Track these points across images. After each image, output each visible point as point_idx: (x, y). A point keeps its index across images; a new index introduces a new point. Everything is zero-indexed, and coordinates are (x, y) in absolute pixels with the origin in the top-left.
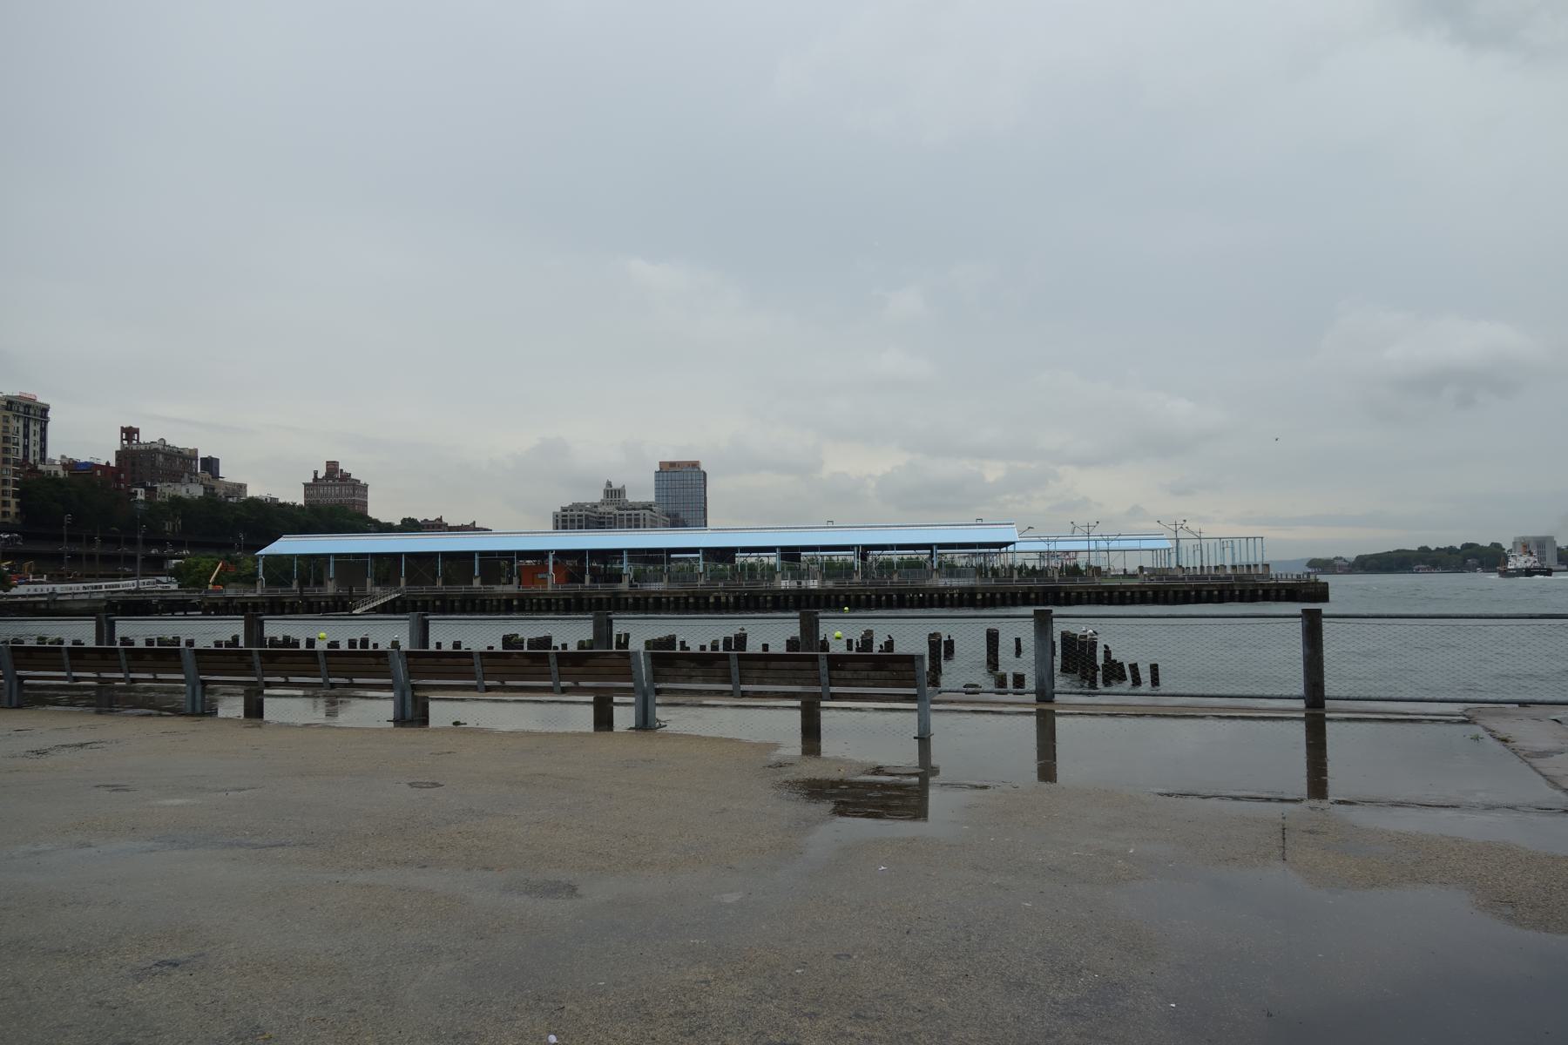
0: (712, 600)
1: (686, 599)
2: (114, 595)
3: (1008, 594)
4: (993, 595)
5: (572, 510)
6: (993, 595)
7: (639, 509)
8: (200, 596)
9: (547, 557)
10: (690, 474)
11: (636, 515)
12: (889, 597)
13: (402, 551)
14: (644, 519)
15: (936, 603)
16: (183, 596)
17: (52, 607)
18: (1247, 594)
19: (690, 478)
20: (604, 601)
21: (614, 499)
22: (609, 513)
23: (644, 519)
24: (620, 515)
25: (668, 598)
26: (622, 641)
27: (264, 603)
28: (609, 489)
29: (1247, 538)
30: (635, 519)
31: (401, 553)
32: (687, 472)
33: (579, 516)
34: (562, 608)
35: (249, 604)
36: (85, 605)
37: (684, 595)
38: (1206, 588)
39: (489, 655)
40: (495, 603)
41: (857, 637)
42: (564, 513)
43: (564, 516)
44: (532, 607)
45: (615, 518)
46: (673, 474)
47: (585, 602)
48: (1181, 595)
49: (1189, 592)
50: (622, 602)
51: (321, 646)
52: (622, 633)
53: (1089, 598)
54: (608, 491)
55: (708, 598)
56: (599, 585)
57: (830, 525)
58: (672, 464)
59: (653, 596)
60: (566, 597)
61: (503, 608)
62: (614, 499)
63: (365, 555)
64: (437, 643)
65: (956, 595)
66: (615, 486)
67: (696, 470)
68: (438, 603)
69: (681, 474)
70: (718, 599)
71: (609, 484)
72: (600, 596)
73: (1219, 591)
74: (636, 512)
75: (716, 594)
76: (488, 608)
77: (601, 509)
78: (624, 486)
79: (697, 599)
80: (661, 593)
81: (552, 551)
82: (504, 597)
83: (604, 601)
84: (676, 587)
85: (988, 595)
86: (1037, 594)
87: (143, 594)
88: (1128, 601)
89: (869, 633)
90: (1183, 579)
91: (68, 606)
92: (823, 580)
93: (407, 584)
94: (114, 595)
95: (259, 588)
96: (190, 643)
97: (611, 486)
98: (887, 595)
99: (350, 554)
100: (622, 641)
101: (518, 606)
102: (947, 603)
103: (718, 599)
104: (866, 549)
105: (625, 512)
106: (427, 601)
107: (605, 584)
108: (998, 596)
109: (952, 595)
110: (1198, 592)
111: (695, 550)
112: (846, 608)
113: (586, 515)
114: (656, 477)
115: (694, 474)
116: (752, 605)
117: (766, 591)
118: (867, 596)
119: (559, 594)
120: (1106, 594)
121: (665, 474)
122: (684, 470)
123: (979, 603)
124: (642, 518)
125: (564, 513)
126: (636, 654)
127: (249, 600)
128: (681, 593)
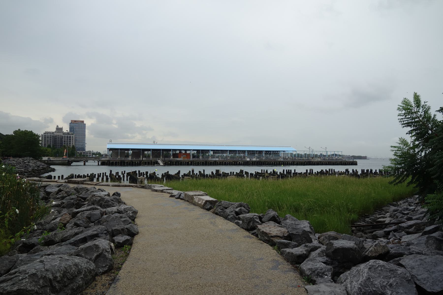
0: (238, 163)
1: (346, 163)
2: (70, 159)
3: (301, 163)
4: (298, 163)
5: (47, 134)
6: (298, 163)
7: (71, 135)
8: (99, 160)
9: (228, 151)
10: (81, 124)
11: (70, 136)
12: (277, 163)
13: (151, 148)
14: (72, 138)
15: (290, 164)
16: (73, 160)
17: (49, 162)
18: (344, 163)
19: (81, 126)
20: (212, 163)
21: (59, 131)
22: (58, 135)
23: (72, 138)
24: (64, 136)
25: (228, 162)
26: (290, 172)
27: (119, 162)
28: (58, 128)
29: (320, 151)
30: (50, 137)
31: (151, 149)
32: (80, 124)
33: (50, 136)
34: (202, 164)
35: (114, 162)
36: (60, 162)
37: (232, 162)
38: (337, 162)
39: (301, 174)
40: (184, 163)
41: (176, 172)
42: (45, 135)
43: (45, 135)
44: (119, 164)
45: (63, 137)
46: (76, 124)
47: (208, 163)
48: (333, 163)
49: (334, 163)
50: (217, 163)
51: (269, 172)
52: (117, 172)
53: (332, 164)
54: (57, 128)
55: (237, 162)
56: (123, 158)
57: (154, 143)
58: (75, 121)
59: (225, 162)
60: (203, 162)
61: (186, 164)
62: (59, 131)
63: (140, 149)
64: (376, 170)
65: (291, 163)
66: (59, 127)
67: (83, 123)
68: (169, 163)
69: (78, 124)
70: (239, 163)
71: (57, 126)
72: (211, 162)
73: (252, 162)
74: (67, 135)
75: (239, 161)
76: (182, 164)
77: (55, 134)
78: (62, 127)
79: (234, 163)
80: (182, 161)
81: (264, 151)
82: (187, 161)
83: (212, 163)
84: (258, 160)
85: (297, 163)
86: (306, 163)
87: (80, 159)
88: (339, 164)
89: (179, 171)
90: (305, 160)
91: (54, 162)
92: (257, 159)
93: (120, 157)
94: (70, 159)
95: (108, 157)
96: (139, 171)
97: (58, 127)
98: (276, 162)
99: (220, 150)
100: (290, 172)
101: (276, 164)
102: (289, 164)
103: (239, 163)
104: (186, 150)
105: (69, 135)
106: (149, 162)
107: (197, 159)
108: (299, 163)
109: (290, 163)
110: (225, 163)
111: (244, 152)
112: (282, 165)
113: (53, 136)
114: (70, 125)
115: (82, 124)
116: (123, 164)
117: (277, 161)
118: (272, 162)
119: (201, 161)
120: (319, 163)
121: (73, 124)
122: (79, 123)
123: (238, 164)
124: (72, 137)
125: (45, 135)
126: (121, 178)
127: (114, 161)
128: (231, 161)
